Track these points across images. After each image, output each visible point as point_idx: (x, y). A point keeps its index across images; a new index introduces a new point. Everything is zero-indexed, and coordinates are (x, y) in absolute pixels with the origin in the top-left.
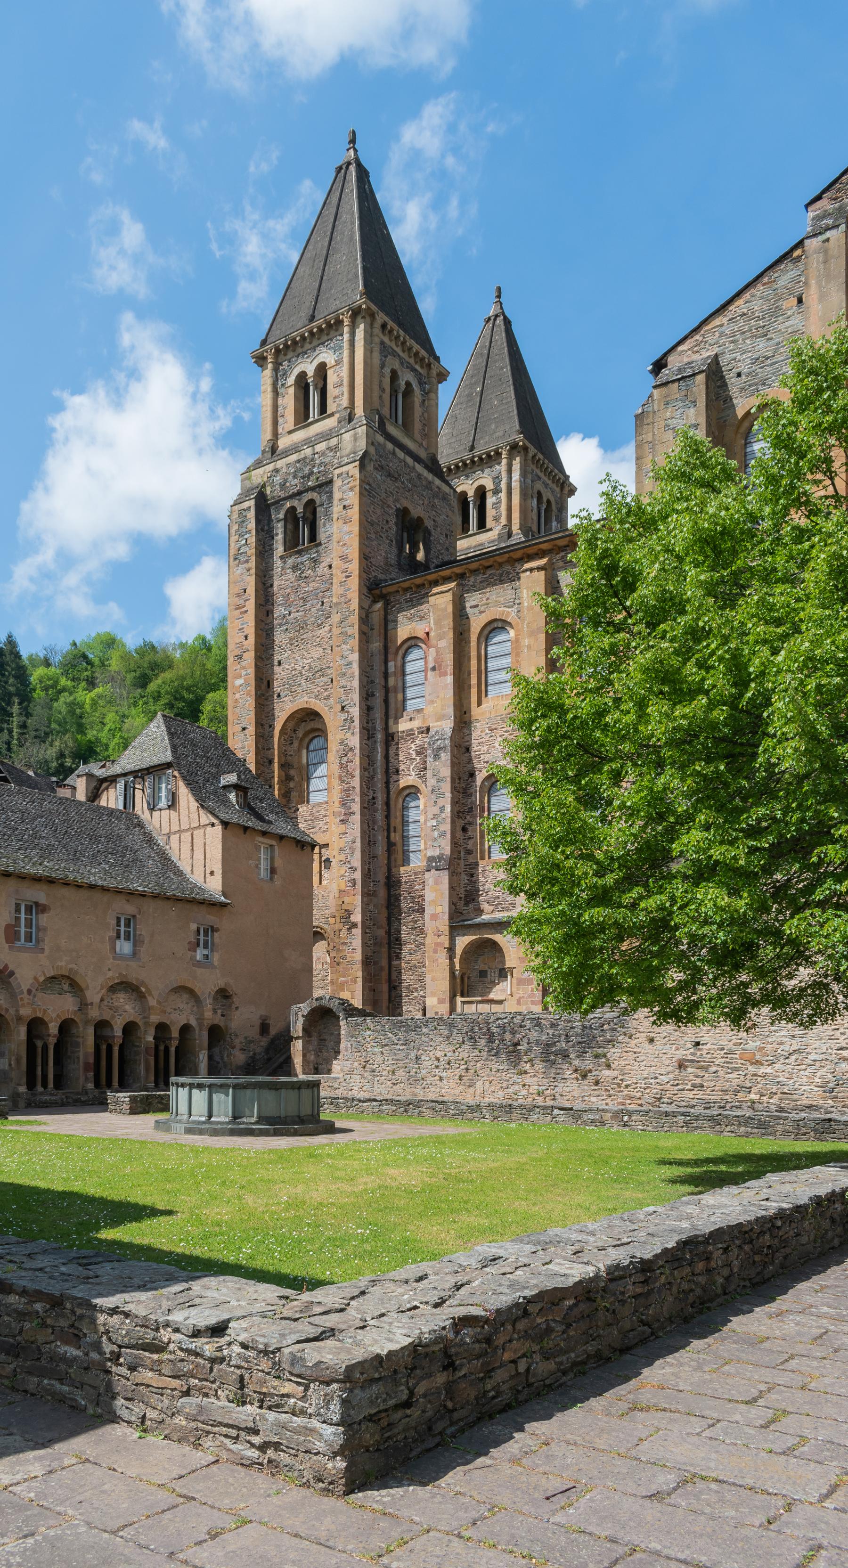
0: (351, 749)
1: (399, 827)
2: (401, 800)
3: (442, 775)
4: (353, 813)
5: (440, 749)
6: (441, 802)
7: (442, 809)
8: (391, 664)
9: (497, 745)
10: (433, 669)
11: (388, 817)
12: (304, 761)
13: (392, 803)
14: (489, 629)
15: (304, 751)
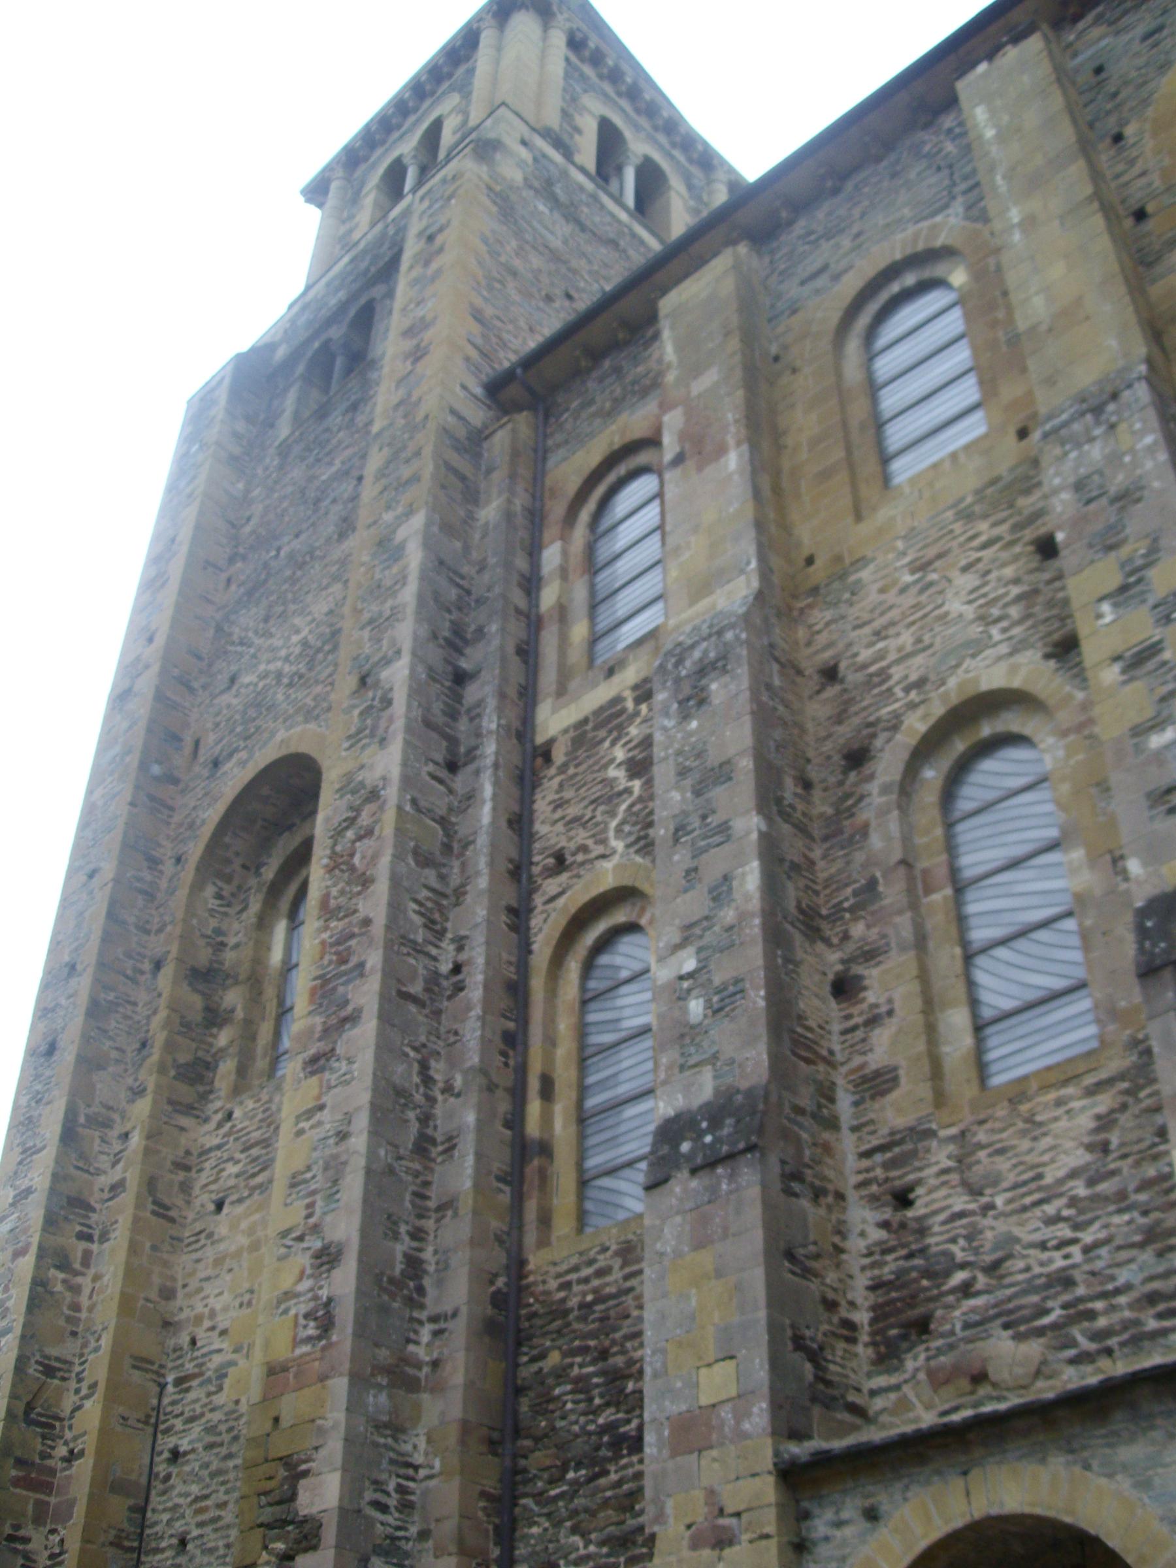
0: (374, 795)
1: (565, 1075)
2: (573, 967)
3: (714, 758)
4: (353, 1019)
5: (704, 670)
6: (714, 864)
7: (721, 892)
8: (551, 556)
9: (955, 606)
10: (679, 460)
11: (513, 1041)
12: (276, 956)
13: (537, 984)
14: (873, 307)
15: (280, 928)
